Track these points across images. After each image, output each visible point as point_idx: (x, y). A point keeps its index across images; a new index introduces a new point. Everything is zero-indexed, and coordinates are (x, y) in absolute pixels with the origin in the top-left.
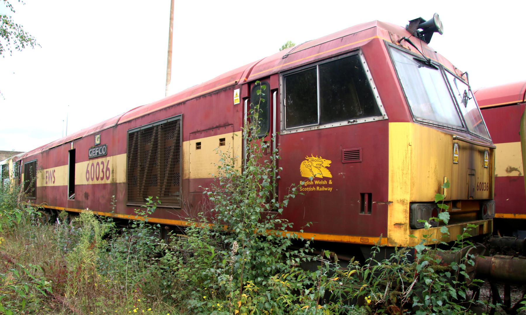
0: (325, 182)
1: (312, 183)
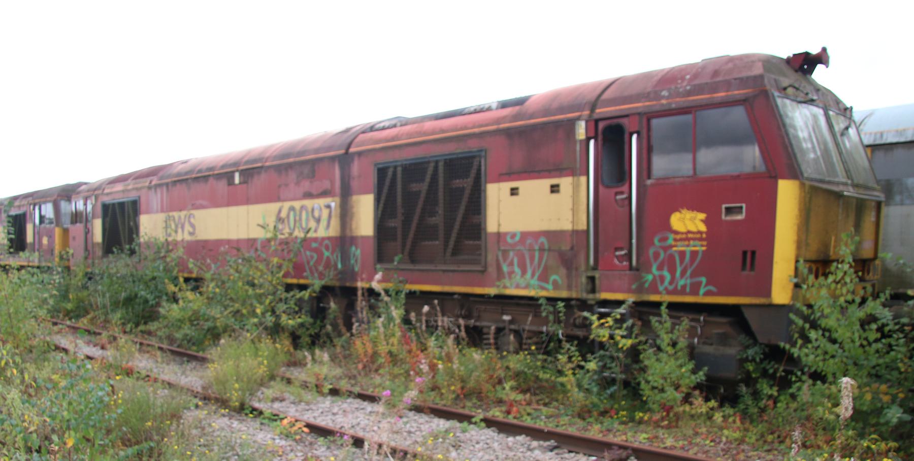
0: (698, 236)
1: (684, 236)
